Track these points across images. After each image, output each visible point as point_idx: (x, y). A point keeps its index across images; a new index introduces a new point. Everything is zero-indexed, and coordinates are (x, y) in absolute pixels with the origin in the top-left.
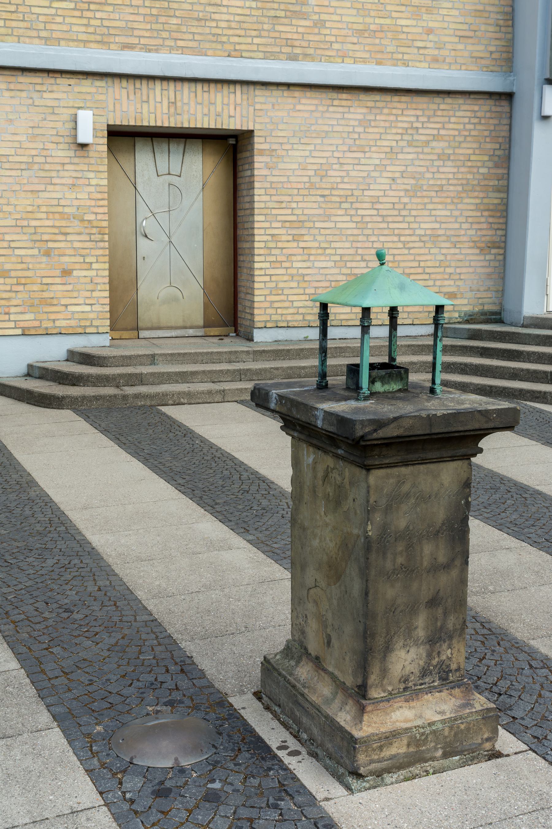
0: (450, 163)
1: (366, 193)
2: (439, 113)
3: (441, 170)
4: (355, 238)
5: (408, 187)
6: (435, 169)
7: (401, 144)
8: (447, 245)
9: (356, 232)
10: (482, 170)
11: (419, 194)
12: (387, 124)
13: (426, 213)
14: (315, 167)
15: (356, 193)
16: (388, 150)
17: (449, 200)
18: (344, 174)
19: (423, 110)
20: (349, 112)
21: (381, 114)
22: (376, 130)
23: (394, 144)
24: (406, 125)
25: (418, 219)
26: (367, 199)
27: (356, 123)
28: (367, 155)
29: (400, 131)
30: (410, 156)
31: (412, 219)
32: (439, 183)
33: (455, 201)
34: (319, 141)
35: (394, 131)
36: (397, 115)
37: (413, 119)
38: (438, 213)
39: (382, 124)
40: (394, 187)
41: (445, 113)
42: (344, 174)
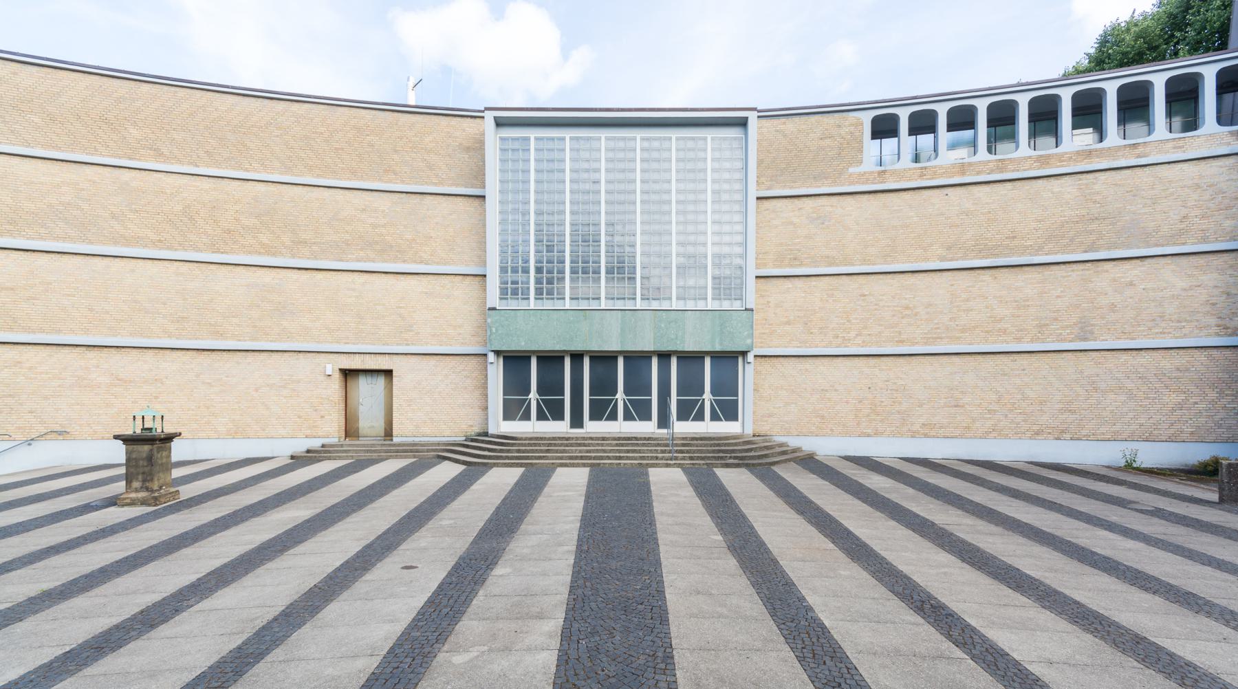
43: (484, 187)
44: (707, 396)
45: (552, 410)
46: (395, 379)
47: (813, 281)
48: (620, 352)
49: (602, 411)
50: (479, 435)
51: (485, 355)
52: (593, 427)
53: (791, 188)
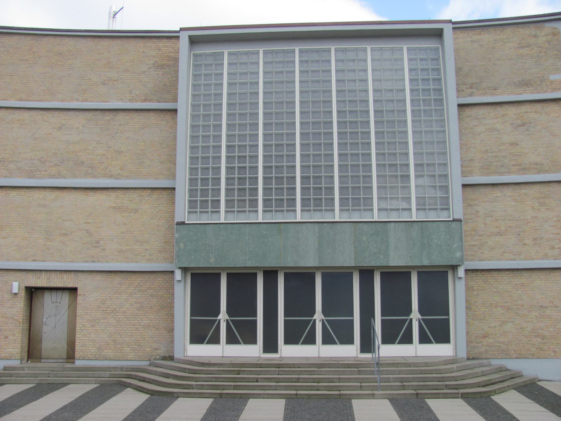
7: (135, 291)
8: (154, 329)
10: (168, 300)
15: (117, 309)
30: (139, 296)
43: (175, 100)
44: (415, 315)
45: (242, 333)
46: (79, 299)
47: (524, 190)
48: (318, 268)
49: (299, 334)
50: (164, 358)
51: (172, 272)
52: (288, 352)
53: (492, 95)
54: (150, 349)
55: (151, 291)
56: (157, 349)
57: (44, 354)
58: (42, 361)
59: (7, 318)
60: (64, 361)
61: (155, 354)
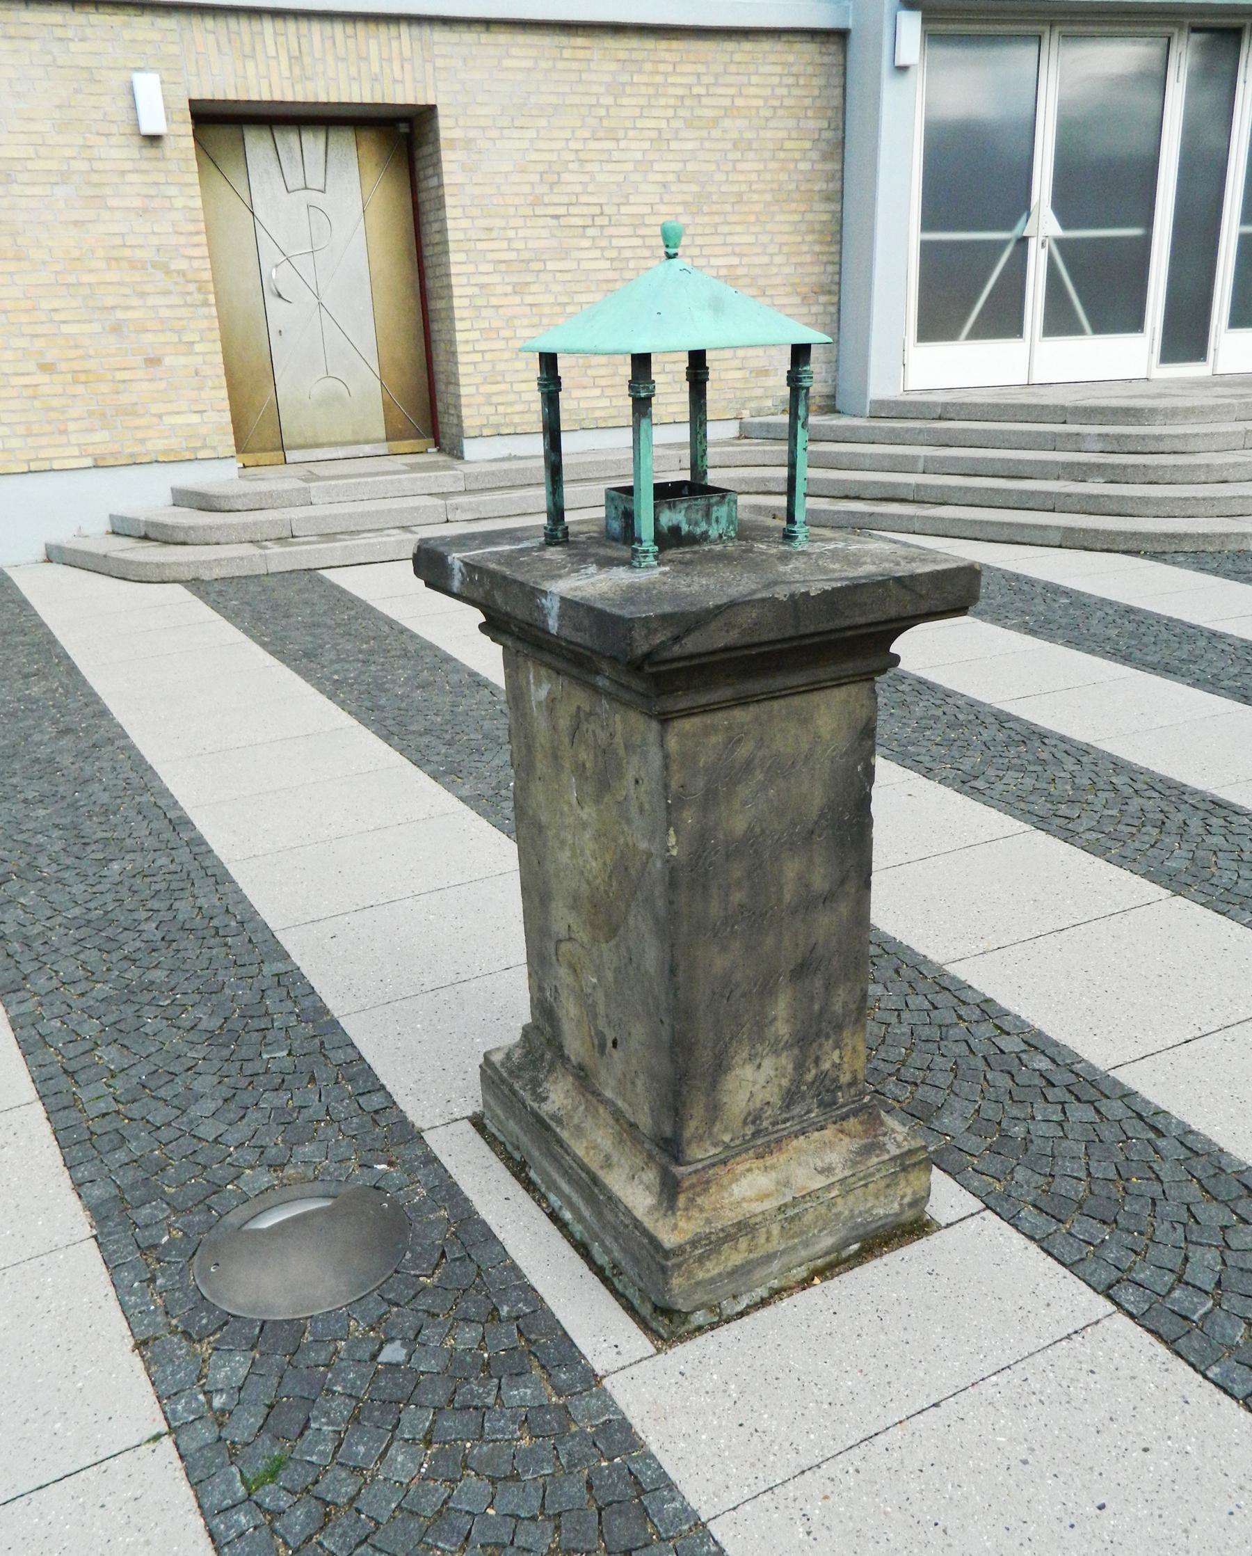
0: (751, 155)
1: (624, 209)
2: (733, 68)
3: (740, 166)
4: (610, 286)
5: (689, 198)
6: (729, 167)
7: (676, 124)
9: (610, 275)
11: (706, 209)
12: (651, 91)
13: (718, 240)
14: (540, 168)
15: (607, 210)
16: (654, 134)
17: (752, 218)
18: (586, 178)
19: (706, 63)
20: (589, 70)
21: (640, 72)
22: (634, 101)
23: (663, 124)
24: (680, 91)
25: (706, 251)
26: (625, 220)
27: (602, 89)
28: (623, 144)
29: (672, 102)
30: (690, 146)
31: (696, 251)
32: (735, 188)
33: (762, 218)
34: (543, 122)
35: (662, 102)
36: (666, 74)
37: (692, 80)
38: (737, 239)
39: (643, 90)
40: (667, 198)
41: (742, 69)
42: (586, 178)
54: (739, 374)
55: (741, 123)
56: (764, 372)
57: (292, 427)
58: (292, 456)
59: (135, 265)
60: (383, 448)
61: (759, 392)
